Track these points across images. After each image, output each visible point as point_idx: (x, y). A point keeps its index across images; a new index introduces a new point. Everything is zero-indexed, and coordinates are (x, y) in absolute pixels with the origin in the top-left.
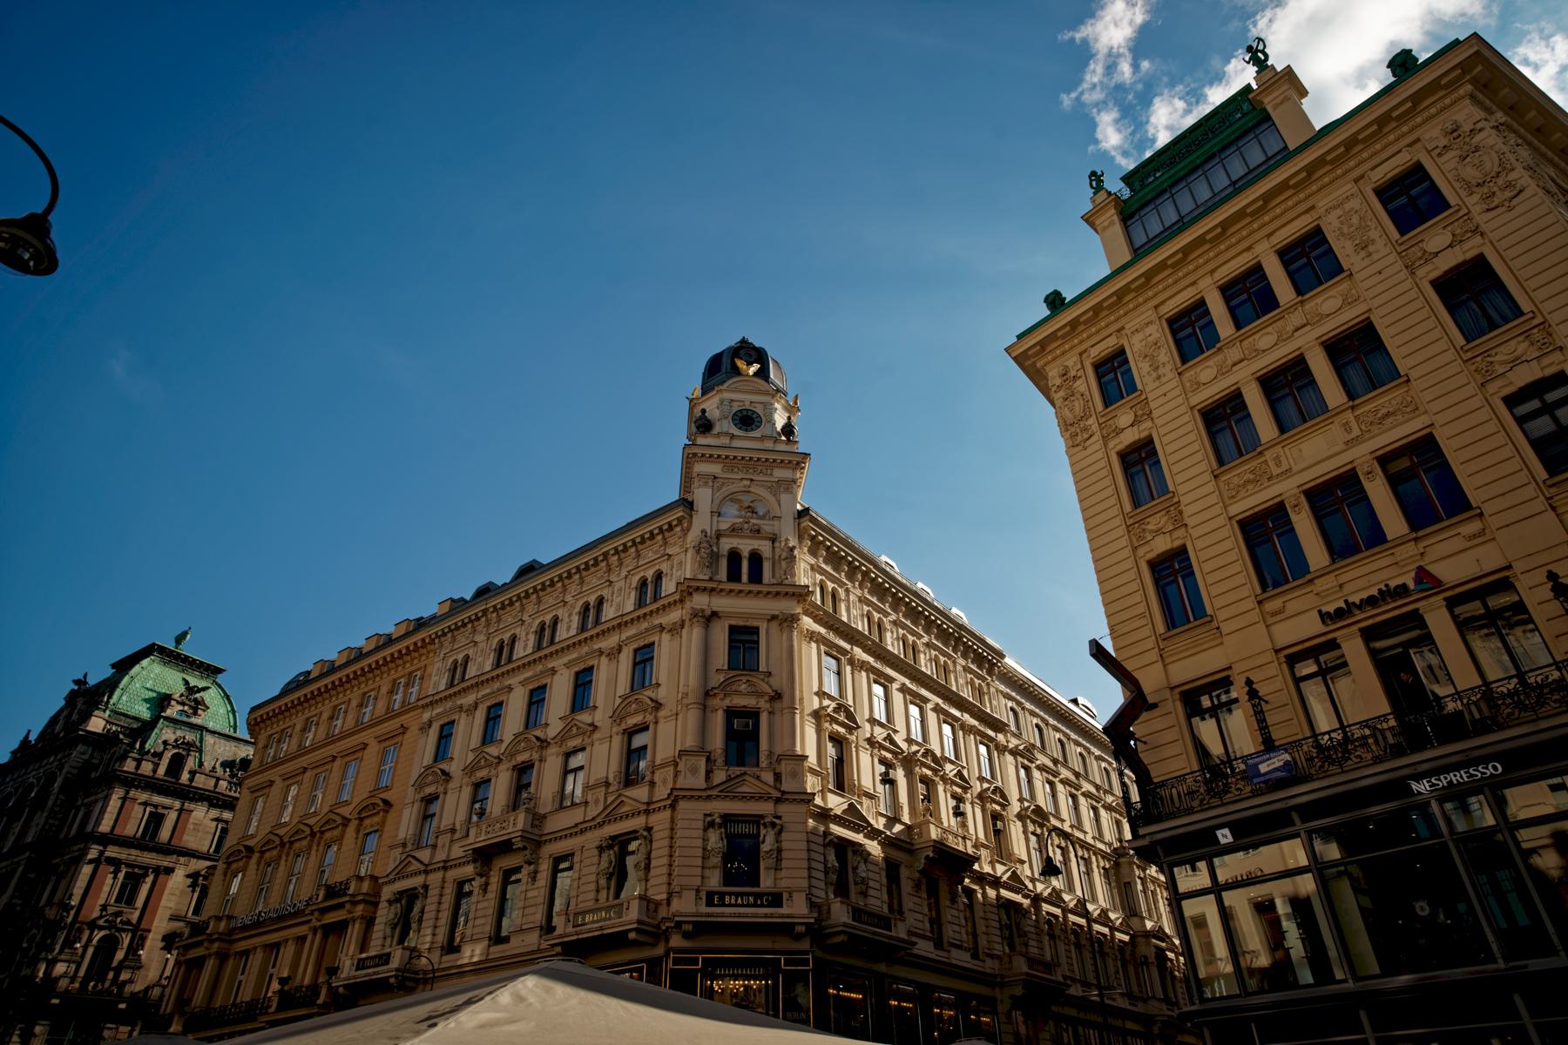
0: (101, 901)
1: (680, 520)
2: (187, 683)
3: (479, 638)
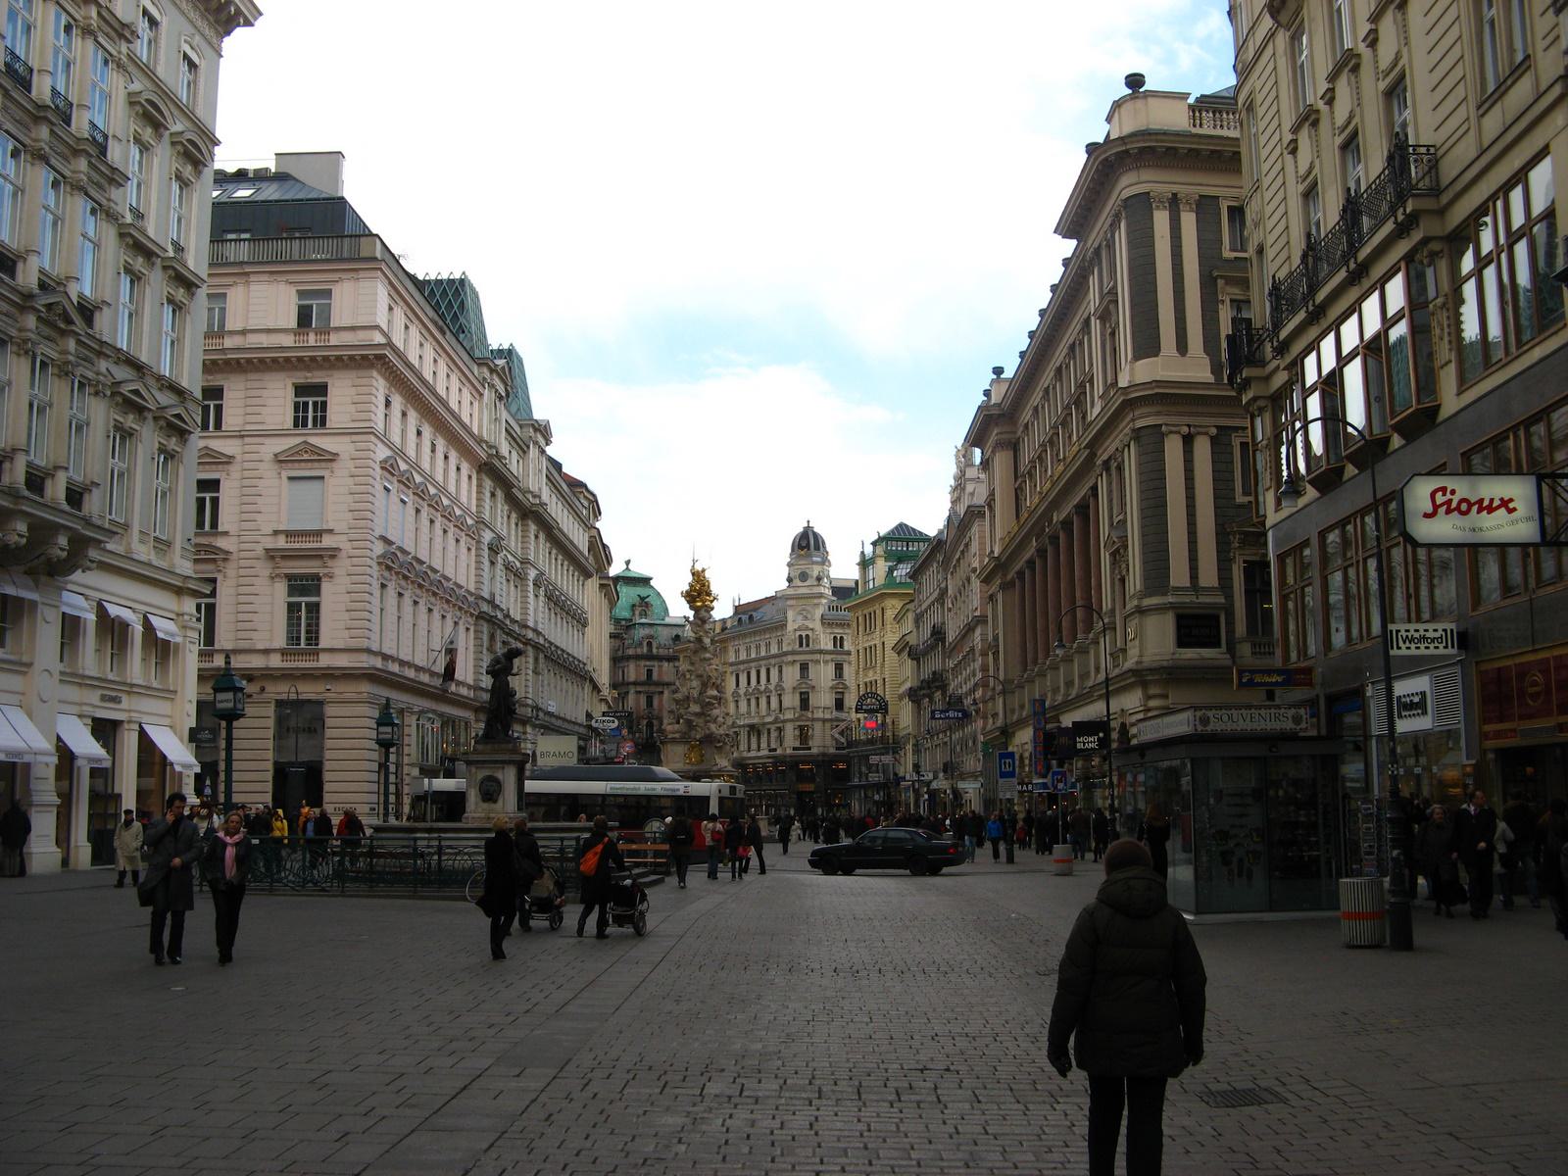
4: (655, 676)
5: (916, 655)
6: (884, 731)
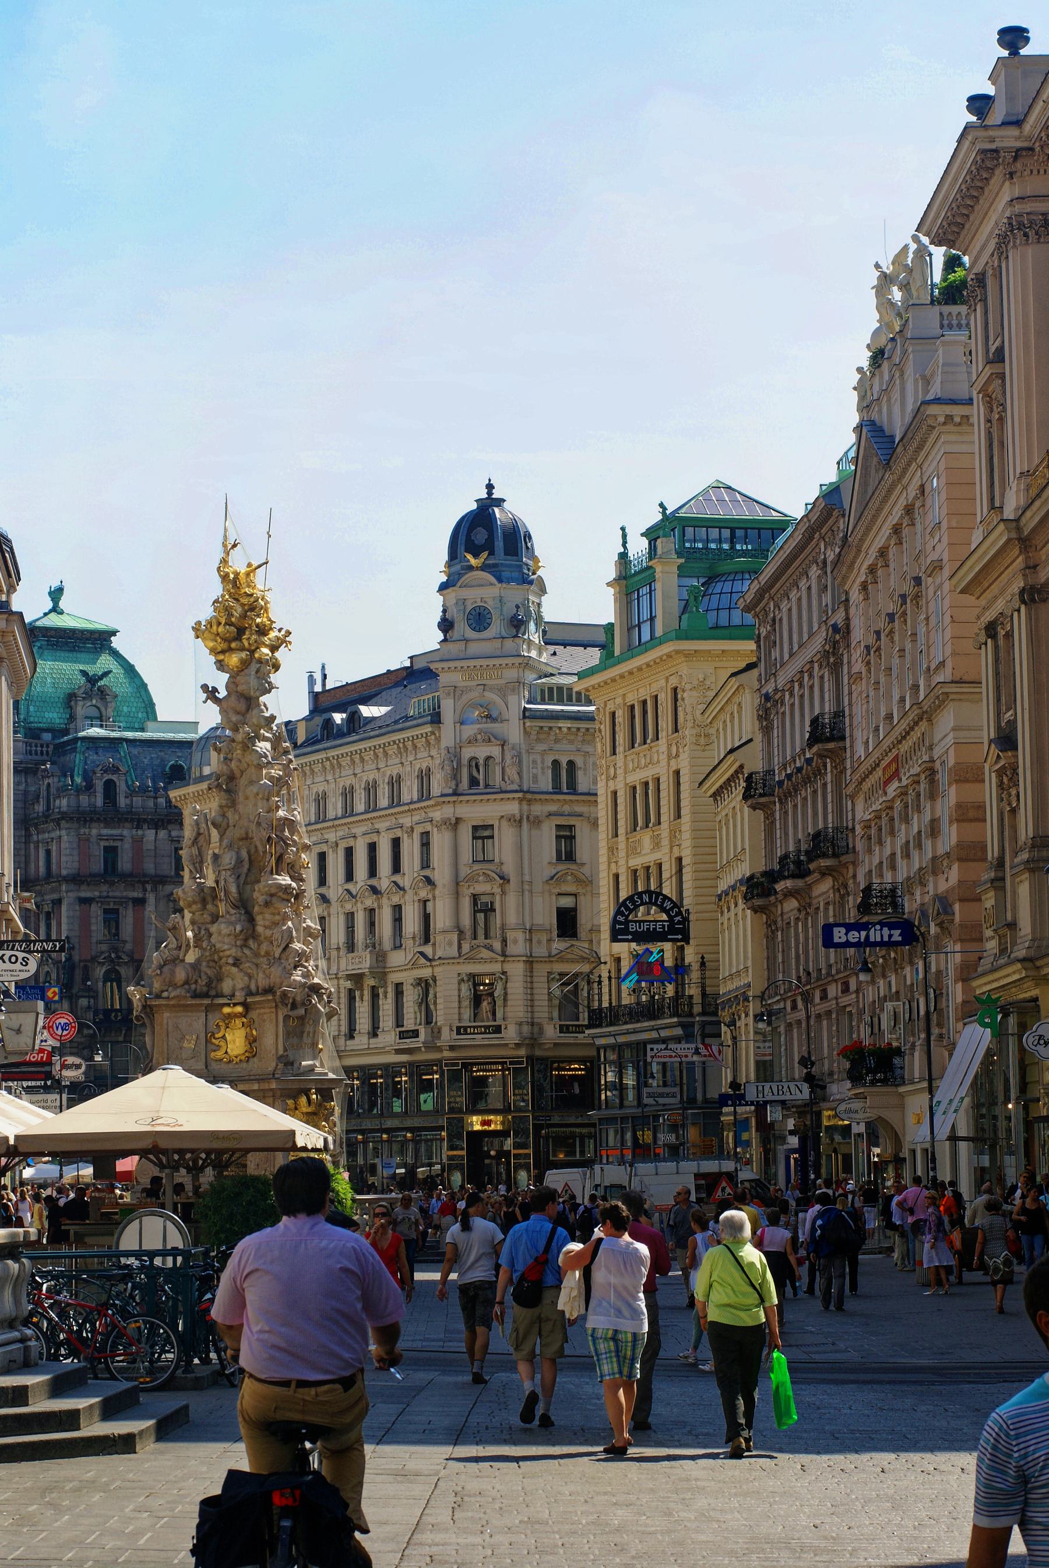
0: (94, 940)
1: (433, 733)
2: (84, 673)
3: (330, 777)
4: (125, 863)
5: (758, 790)
6: (680, 986)
